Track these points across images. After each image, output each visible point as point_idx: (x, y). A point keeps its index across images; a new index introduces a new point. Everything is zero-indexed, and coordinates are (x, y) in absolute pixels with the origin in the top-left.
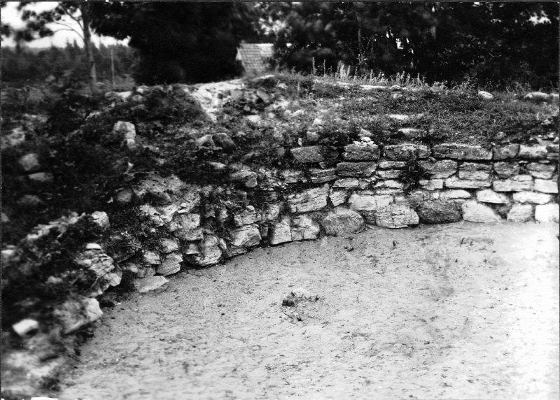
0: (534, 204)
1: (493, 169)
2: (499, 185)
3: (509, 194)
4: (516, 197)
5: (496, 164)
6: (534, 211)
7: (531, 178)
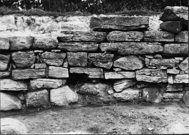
0: (49, 89)
1: (11, 57)
2: (16, 73)
3: (27, 81)
4: (34, 83)
5: (14, 54)
6: (49, 95)
7: (45, 66)
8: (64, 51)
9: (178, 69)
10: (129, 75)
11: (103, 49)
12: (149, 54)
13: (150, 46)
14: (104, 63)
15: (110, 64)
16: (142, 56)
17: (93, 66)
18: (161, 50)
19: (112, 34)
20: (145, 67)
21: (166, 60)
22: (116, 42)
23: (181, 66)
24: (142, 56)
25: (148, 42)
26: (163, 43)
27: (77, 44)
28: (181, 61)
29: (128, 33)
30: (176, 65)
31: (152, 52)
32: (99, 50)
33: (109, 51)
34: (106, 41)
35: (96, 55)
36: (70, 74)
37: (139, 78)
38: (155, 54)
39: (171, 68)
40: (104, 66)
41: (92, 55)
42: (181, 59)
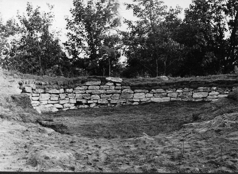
3: (62, 104)
5: (60, 94)
8: (75, 93)
9: (111, 98)
10: (96, 101)
11: (87, 92)
12: (102, 94)
13: (102, 91)
14: (87, 97)
15: (89, 97)
16: (99, 94)
17: (84, 98)
18: (106, 92)
19: (90, 87)
20: (101, 98)
21: (107, 96)
22: (91, 90)
23: (112, 97)
24: (99, 94)
25: (101, 89)
26: (106, 90)
27: (79, 91)
28: (112, 96)
29: (95, 86)
30: (110, 97)
31: (103, 93)
32: (85, 93)
33: (89, 93)
34: (87, 89)
35: (84, 94)
36: (76, 101)
37: (99, 102)
38: (104, 93)
39: (109, 98)
40: (87, 98)
41: (83, 94)
42: (112, 95)
